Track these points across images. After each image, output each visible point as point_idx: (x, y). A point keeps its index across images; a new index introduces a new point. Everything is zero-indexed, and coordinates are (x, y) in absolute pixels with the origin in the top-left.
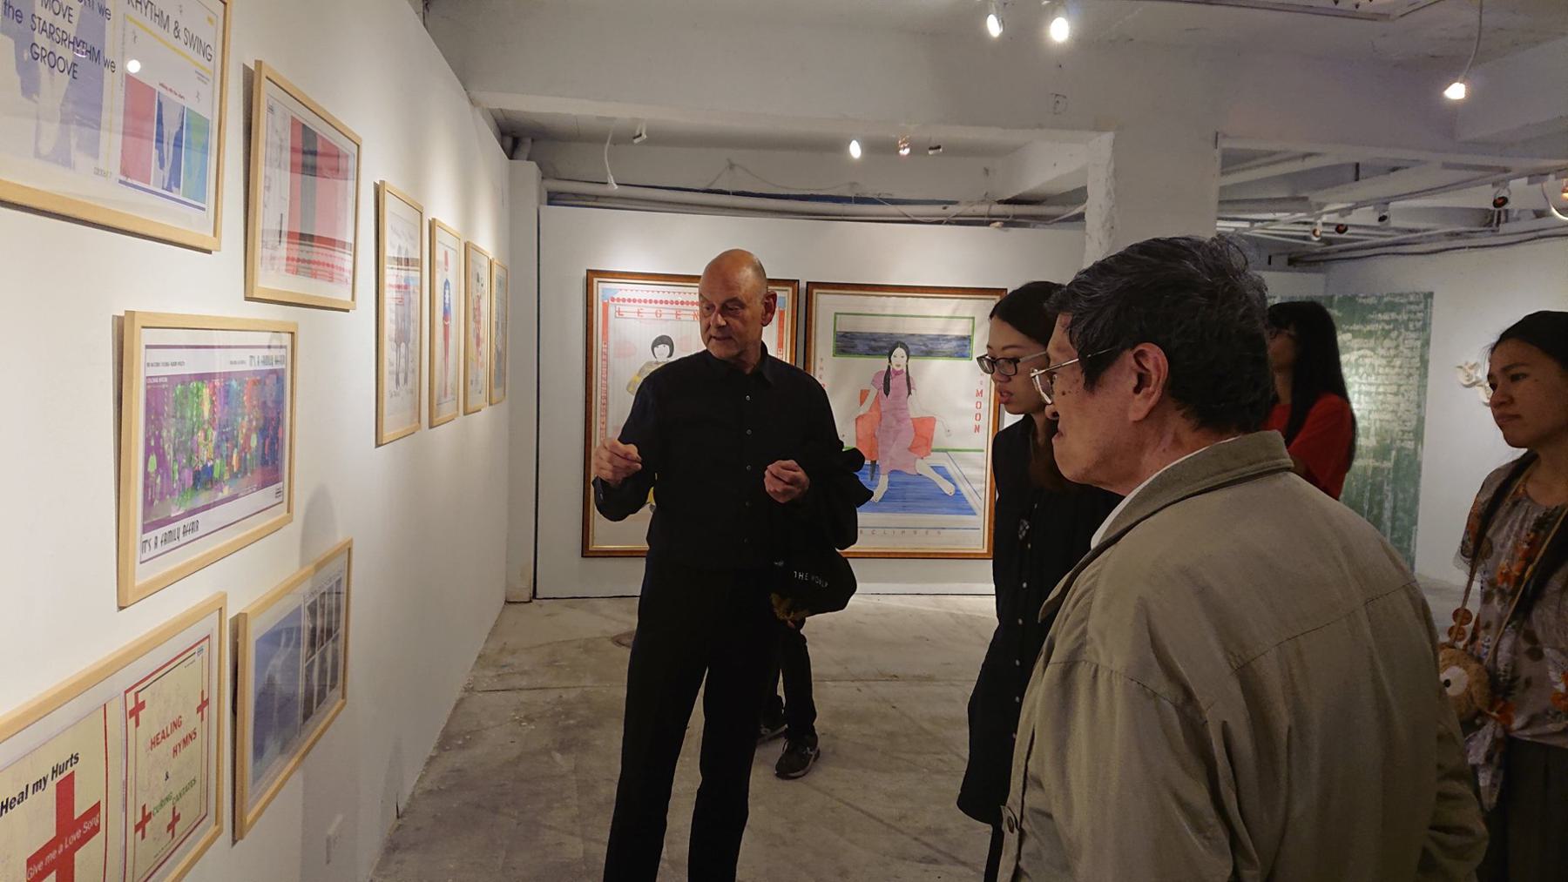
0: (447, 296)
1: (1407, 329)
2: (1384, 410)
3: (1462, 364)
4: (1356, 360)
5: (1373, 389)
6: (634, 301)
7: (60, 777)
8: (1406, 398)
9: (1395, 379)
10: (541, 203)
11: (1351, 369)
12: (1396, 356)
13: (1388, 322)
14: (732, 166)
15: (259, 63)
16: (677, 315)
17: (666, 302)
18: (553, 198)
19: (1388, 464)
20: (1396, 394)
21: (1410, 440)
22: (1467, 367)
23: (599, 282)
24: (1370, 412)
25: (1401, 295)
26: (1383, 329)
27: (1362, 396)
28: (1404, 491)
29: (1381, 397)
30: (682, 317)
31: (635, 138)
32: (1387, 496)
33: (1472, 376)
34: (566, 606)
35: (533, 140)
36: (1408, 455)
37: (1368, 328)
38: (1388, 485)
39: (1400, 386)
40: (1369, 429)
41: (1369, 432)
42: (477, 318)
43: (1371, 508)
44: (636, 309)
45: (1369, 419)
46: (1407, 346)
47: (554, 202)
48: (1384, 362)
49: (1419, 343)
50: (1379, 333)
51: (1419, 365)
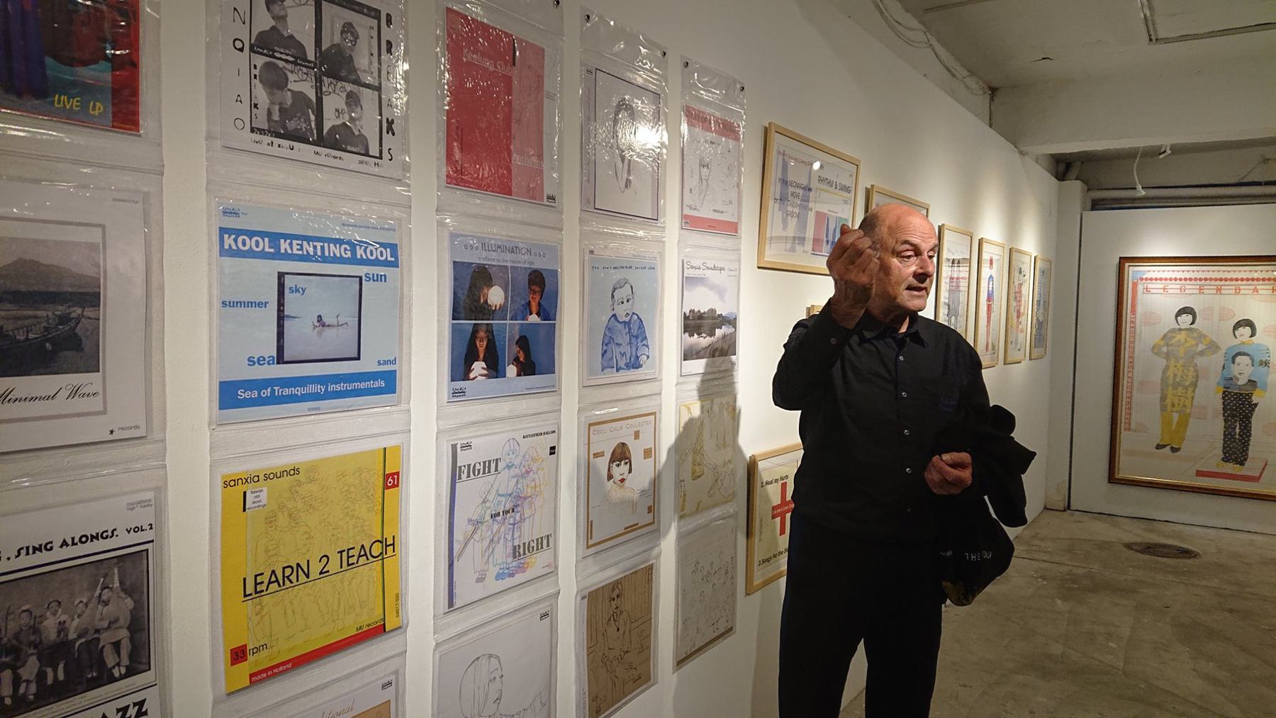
0: (991, 286)
6: (1161, 279)
7: (782, 482)
10: (1084, 209)
14: (1266, 161)
15: (872, 186)
16: (1200, 289)
17: (1190, 279)
18: (1096, 205)
23: (1129, 266)
30: (1205, 291)
31: (1160, 154)
34: (1094, 518)
35: (1082, 163)
42: (1018, 299)
44: (1162, 286)
47: (1097, 207)
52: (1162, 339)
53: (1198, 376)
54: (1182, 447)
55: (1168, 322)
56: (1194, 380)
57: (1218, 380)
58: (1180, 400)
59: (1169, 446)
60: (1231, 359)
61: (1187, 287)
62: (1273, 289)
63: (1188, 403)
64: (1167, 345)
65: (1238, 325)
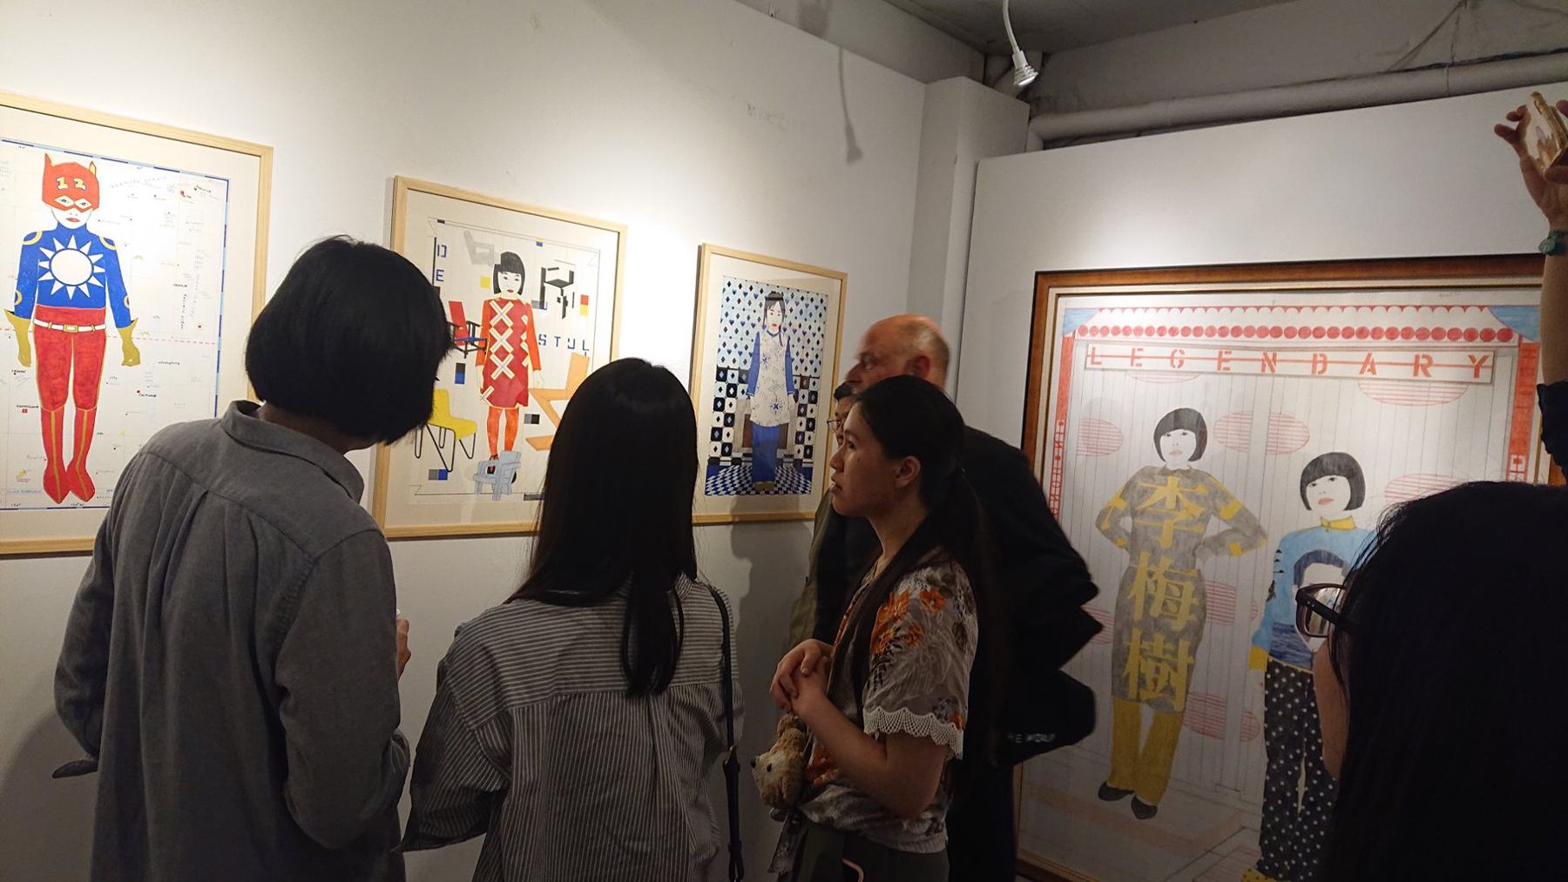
6: (1127, 331)
16: (1220, 360)
23: (1059, 295)
30: (1234, 367)
44: (1127, 350)
52: (1123, 496)
53: (1204, 609)
54: (1159, 806)
55: (1138, 452)
56: (1193, 618)
57: (1256, 626)
58: (1158, 670)
59: (1129, 798)
60: (1291, 573)
61: (1189, 352)
62: (1416, 365)
63: (1178, 682)
64: (1134, 514)
65: (1316, 470)
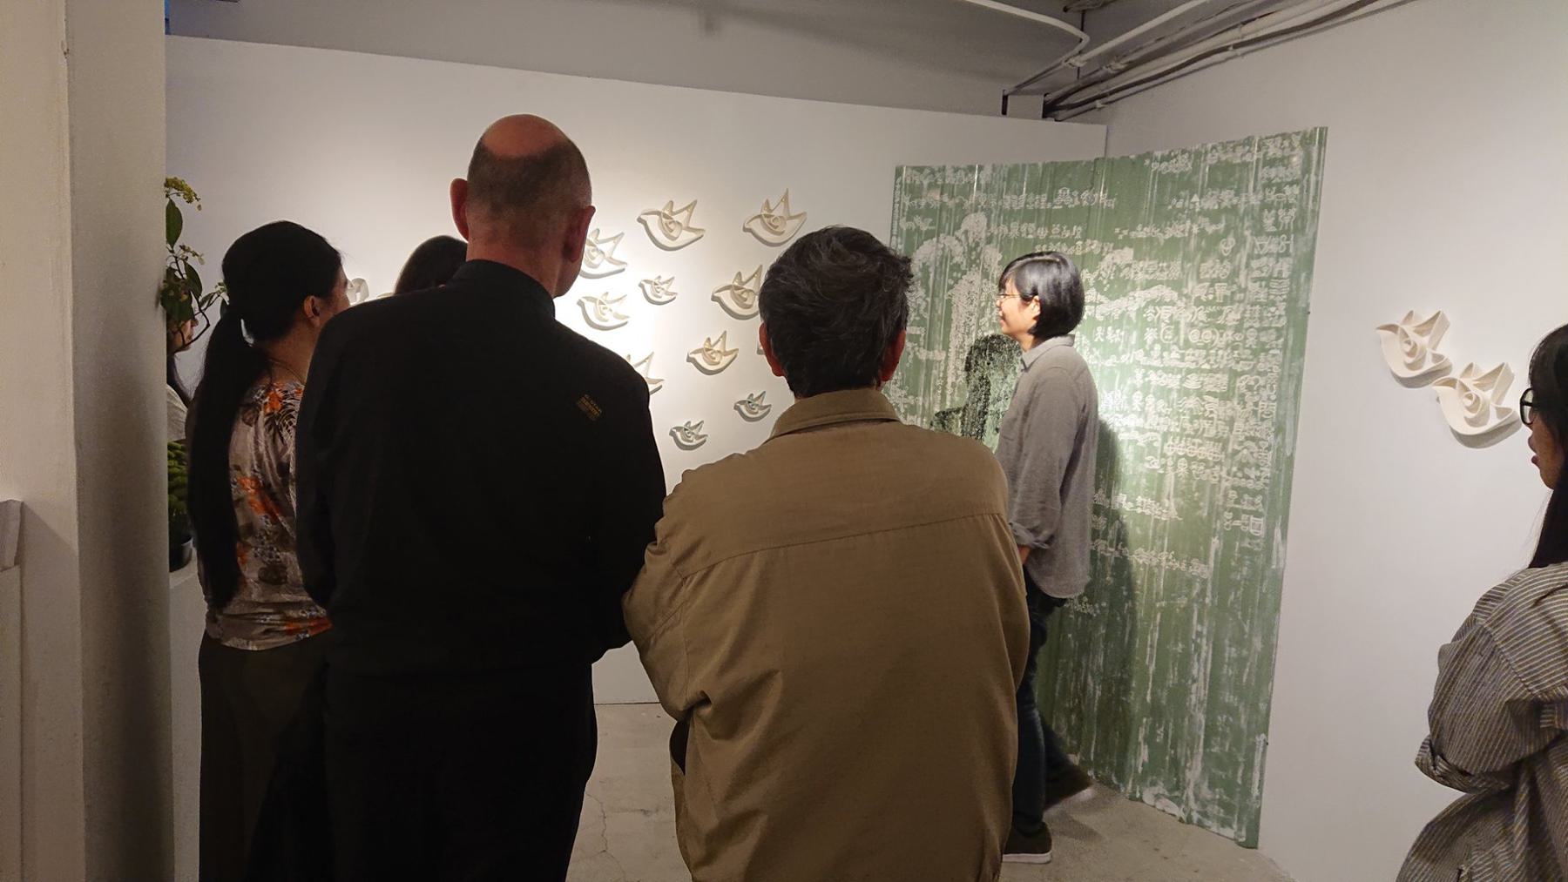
1: (1259, 231)
2: (1197, 433)
3: (1397, 320)
4: (1140, 311)
5: (1173, 382)
8: (1250, 406)
9: (1224, 358)
11: (1129, 332)
12: (1229, 300)
13: (1214, 217)
19: (1203, 570)
20: (1225, 397)
21: (1257, 514)
22: (1409, 329)
24: (1165, 436)
25: (1248, 142)
26: (1202, 233)
27: (1150, 399)
28: (1241, 641)
29: (1192, 402)
32: (1198, 648)
33: (1423, 351)
36: (1250, 552)
37: (1170, 232)
38: (1200, 621)
39: (1234, 375)
40: (1162, 476)
41: (1160, 490)
43: (1161, 673)
45: (1163, 455)
46: (1256, 274)
48: (1202, 316)
49: (1285, 266)
50: (1193, 243)
51: (1283, 321)
